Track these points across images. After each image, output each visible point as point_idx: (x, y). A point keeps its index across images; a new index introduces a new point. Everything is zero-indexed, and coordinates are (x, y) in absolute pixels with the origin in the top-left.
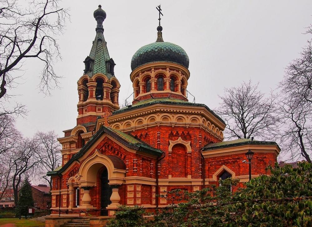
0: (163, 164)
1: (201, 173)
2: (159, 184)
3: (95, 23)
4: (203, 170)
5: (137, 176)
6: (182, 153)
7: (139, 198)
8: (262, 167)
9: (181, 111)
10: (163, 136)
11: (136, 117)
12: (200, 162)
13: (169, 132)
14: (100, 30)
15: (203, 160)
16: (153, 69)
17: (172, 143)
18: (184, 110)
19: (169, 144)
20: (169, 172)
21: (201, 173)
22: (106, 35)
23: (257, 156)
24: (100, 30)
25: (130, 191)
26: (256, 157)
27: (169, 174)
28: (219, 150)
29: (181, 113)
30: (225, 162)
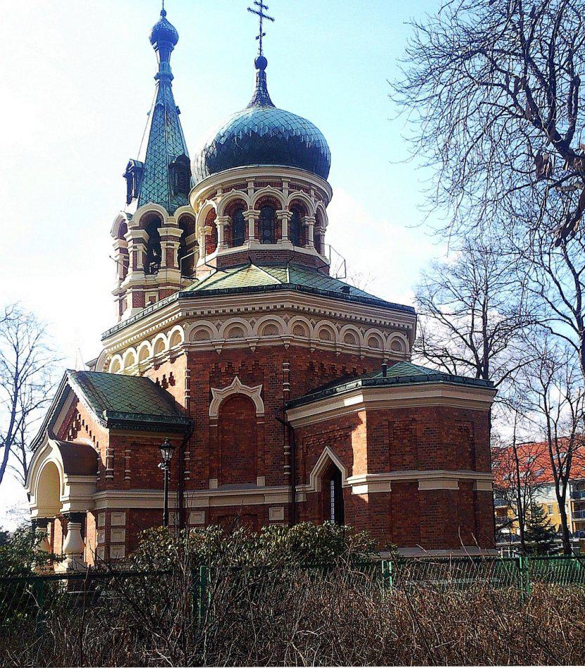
0: (198, 451)
1: (289, 470)
2: (188, 504)
3: (152, 59)
4: (292, 460)
5: (112, 489)
6: (247, 418)
7: (120, 543)
8: (408, 449)
9: (235, 310)
10: (196, 380)
11: (255, 313)
12: (286, 439)
13: (210, 368)
14: (165, 78)
15: (291, 433)
16: (251, 185)
17: (218, 395)
18: (247, 305)
19: (211, 398)
20: (212, 471)
21: (289, 470)
22: (181, 93)
23: (389, 418)
24: (165, 78)
25: (118, 527)
26: (387, 423)
27: (211, 477)
28: (315, 407)
29: (235, 315)
30: (329, 439)
